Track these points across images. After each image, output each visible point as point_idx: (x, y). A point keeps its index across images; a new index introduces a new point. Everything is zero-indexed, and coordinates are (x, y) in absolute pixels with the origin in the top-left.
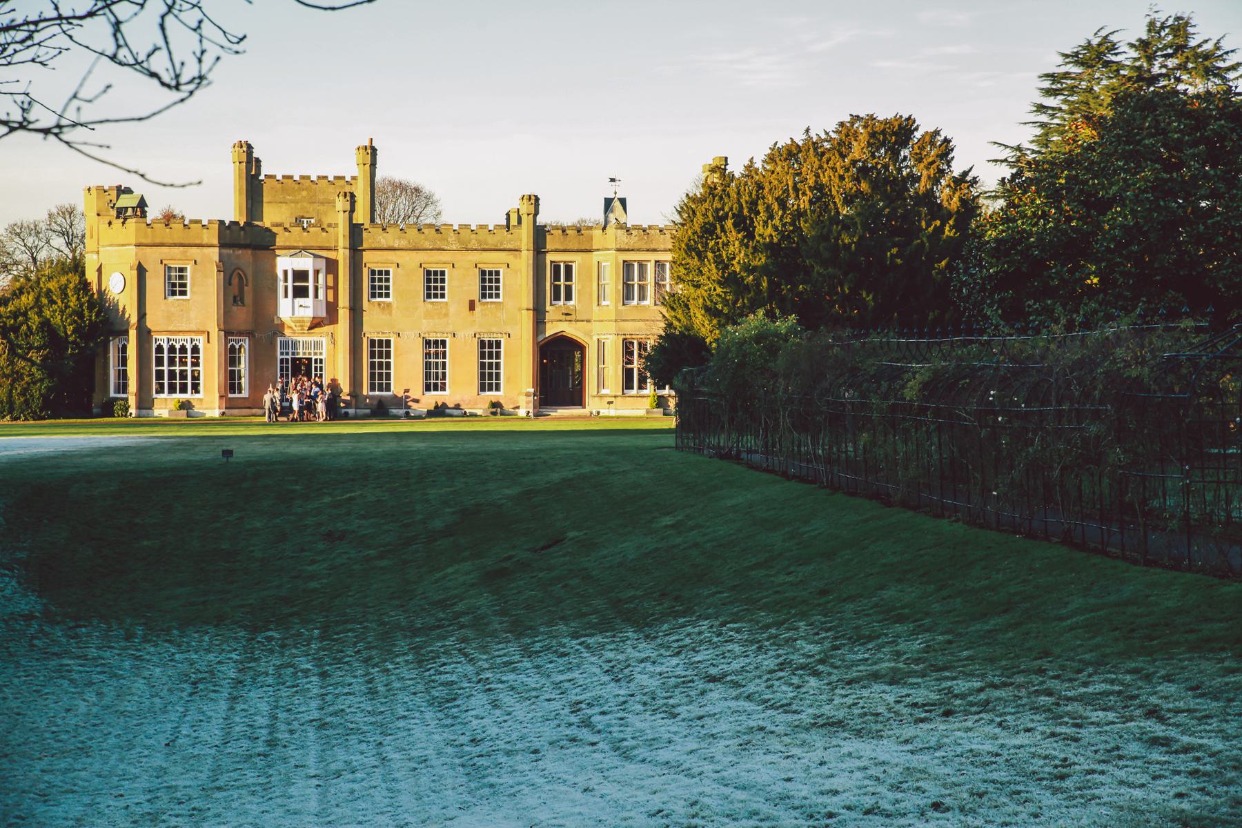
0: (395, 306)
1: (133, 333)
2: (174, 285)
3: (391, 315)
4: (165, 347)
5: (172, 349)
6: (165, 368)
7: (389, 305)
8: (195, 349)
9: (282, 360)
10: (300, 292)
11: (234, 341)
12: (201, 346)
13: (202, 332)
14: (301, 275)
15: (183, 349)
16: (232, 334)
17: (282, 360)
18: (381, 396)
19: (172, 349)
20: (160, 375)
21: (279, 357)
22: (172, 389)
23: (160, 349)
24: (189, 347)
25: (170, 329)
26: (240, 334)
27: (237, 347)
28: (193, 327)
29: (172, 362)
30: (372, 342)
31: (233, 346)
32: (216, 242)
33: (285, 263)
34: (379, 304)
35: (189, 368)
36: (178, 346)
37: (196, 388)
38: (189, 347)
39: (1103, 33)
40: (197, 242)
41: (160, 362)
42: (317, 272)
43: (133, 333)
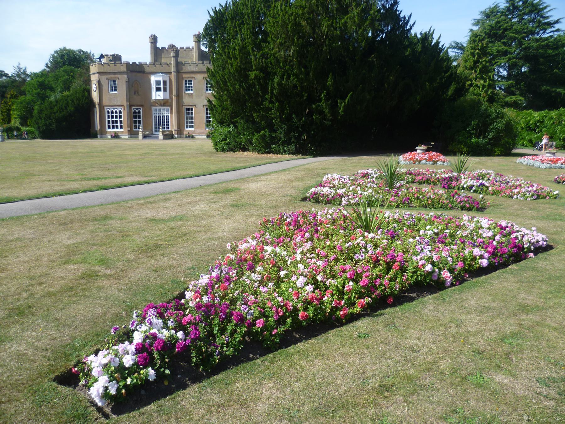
0: (194, 94)
1: (97, 106)
2: (112, 87)
3: (192, 98)
4: (110, 111)
5: (112, 112)
6: (110, 119)
7: (192, 94)
8: (120, 112)
9: (155, 116)
10: (158, 89)
11: (134, 109)
12: (122, 111)
13: (122, 106)
14: (158, 83)
15: (116, 112)
16: (134, 106)
17: (155, 116)
18: (190, 131)
19: (112, 112)
20: (109, 121)
21: (153, 115)
22: (113, 127)
23: (108, 112)
24: (118, 111)
25: (111, 104)
26: (138, 106)
27: (137, 111)
28: (119, 103)
29: (112, 117)
30: (187, 109)
31: (135, 112)
32: (125, 70)
33: (153, 79)
34: (188, 94)
35: (118, 119)
36: (114, 111)
37: (121, 127)
38: (118, 111)
39: (496, 4)
40: (119, 70)
41: (109, 117)
42: (165, 82)
43: (97, 106)
